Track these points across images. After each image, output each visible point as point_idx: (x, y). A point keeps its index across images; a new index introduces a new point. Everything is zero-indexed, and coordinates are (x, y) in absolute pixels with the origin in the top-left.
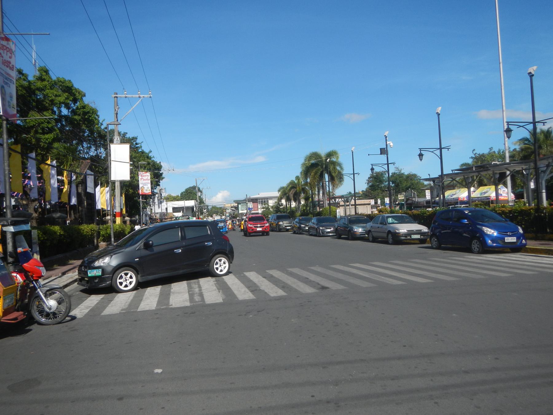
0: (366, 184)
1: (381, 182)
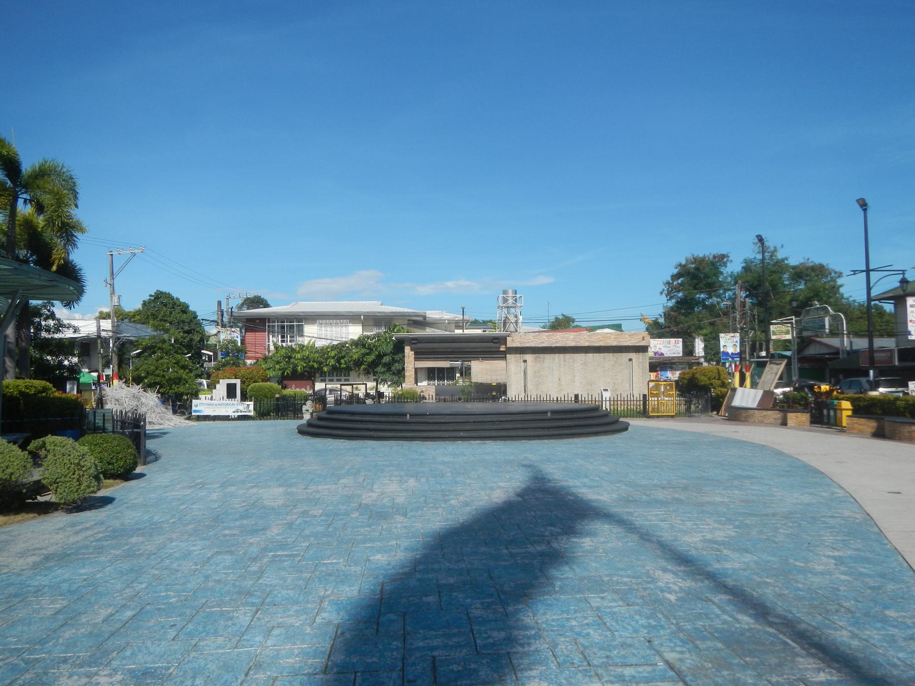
0: (664, 295)
1: (711, 287)
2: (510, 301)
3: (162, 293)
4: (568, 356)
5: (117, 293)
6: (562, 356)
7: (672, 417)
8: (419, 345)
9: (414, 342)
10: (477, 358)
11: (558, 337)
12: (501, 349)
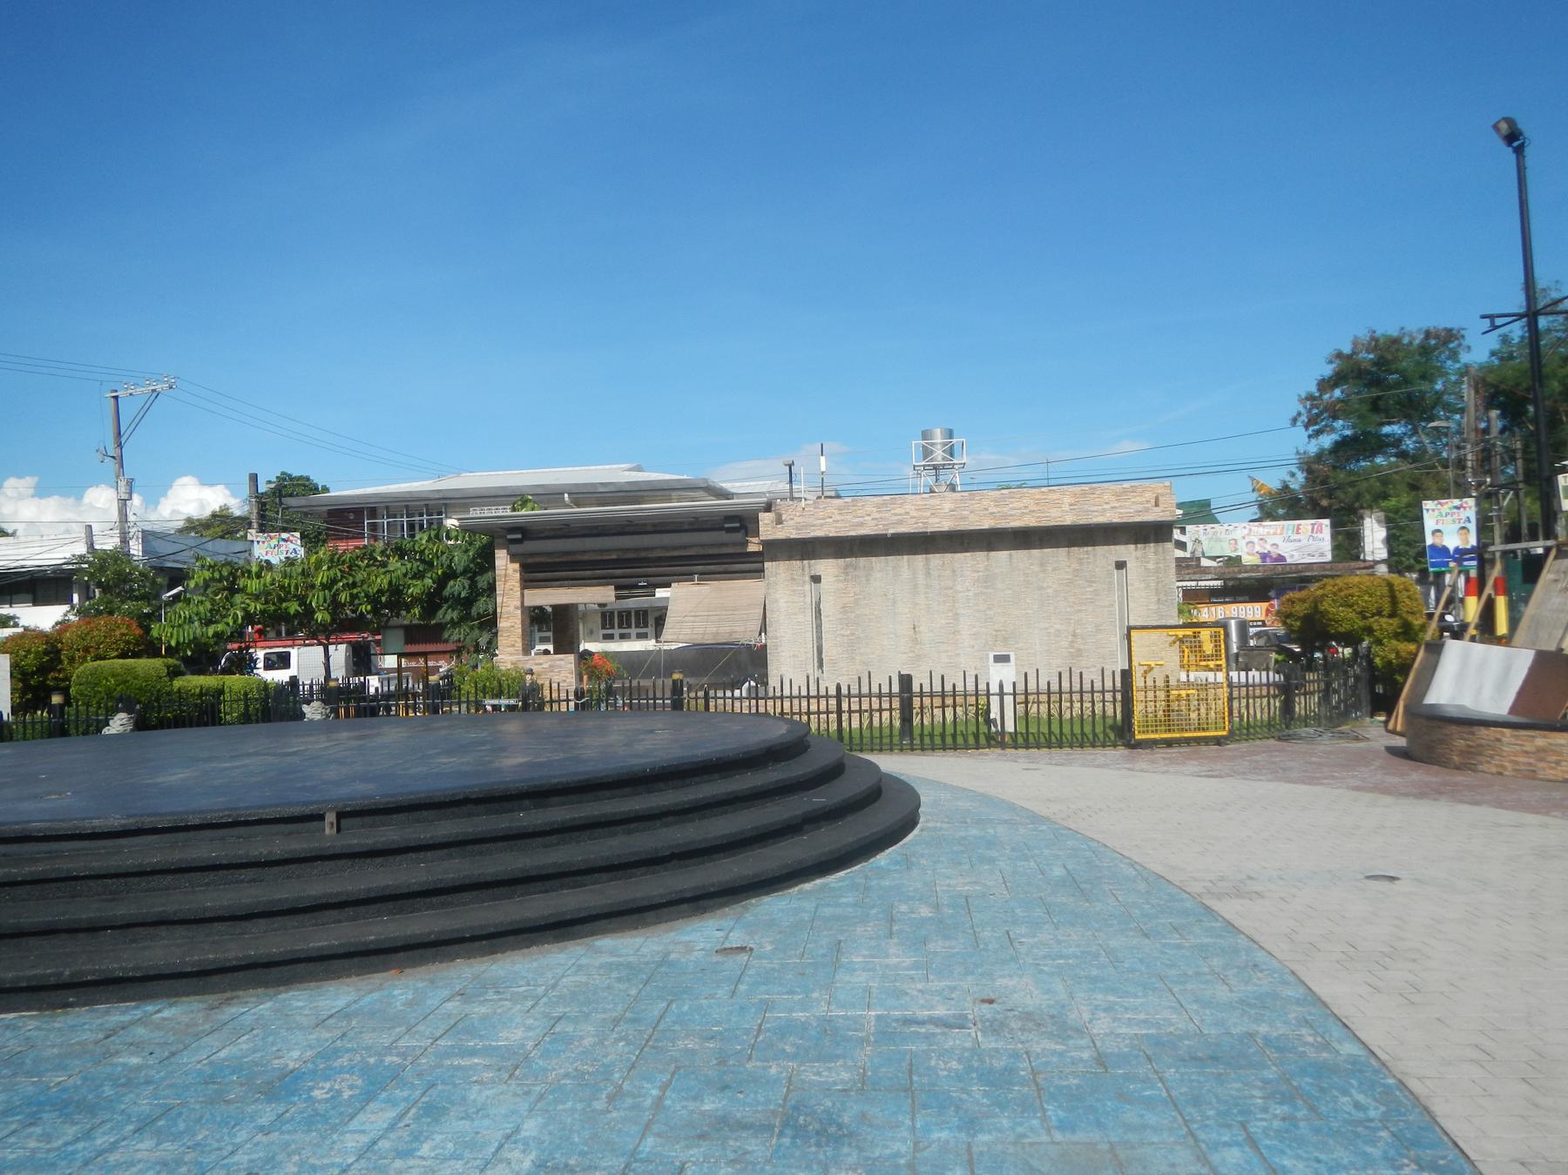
2: (939, 455)
3: (290, 475)
4: (936, 559)
5: (129, 471)
6: (919, 559)
7: (1218, 741)
8: (530, 546)
9: (518, 535)
10: (686, 576)
11: (908, 507)
12: (752, 548)
